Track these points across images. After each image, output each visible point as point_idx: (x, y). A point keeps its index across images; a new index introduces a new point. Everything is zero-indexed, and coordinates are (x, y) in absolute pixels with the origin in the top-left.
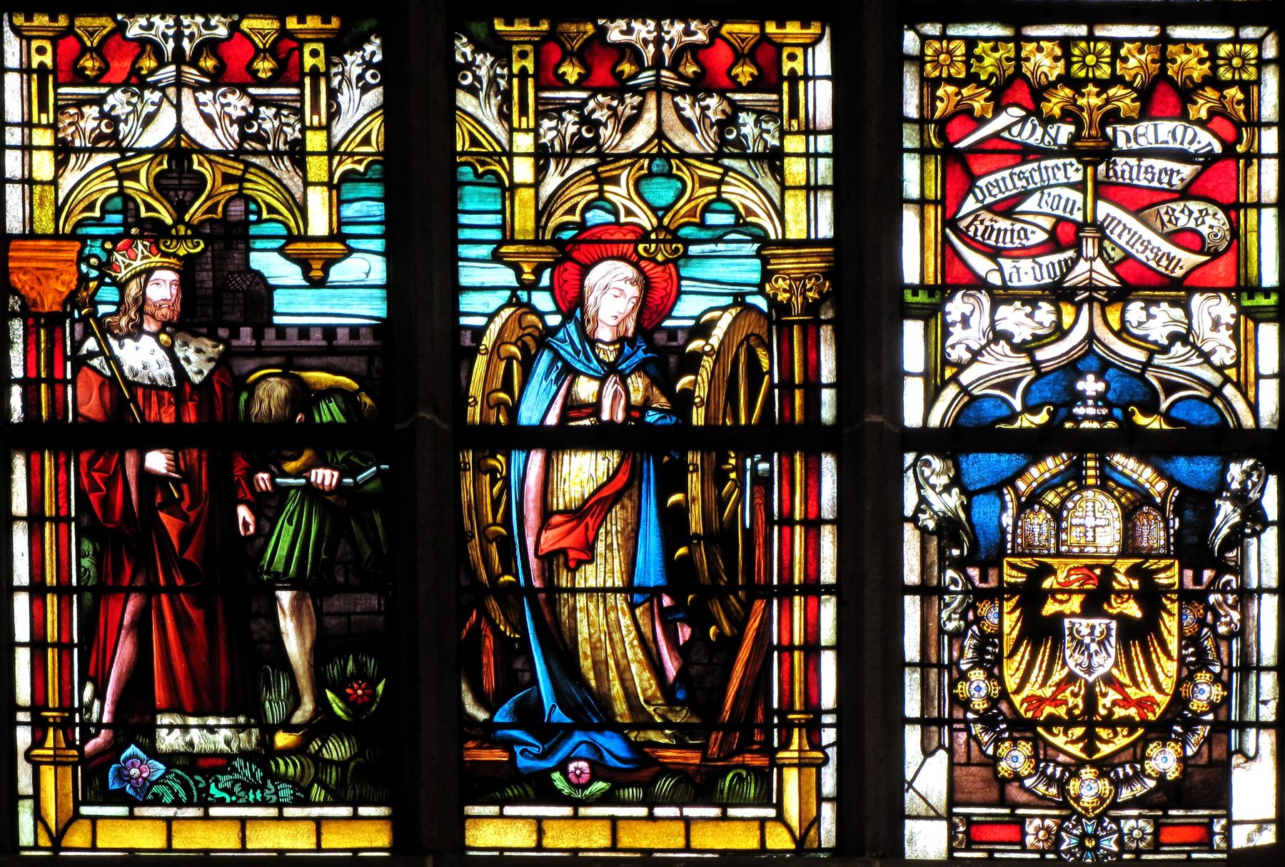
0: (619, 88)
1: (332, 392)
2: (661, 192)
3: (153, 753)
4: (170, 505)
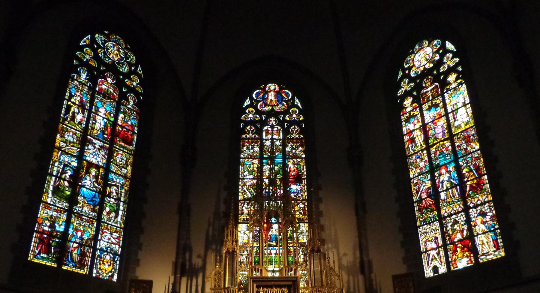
0: (83, 221)
1: (59, 235)
2: (84, 228)
3: (40, 256)
4: (46, 239)
